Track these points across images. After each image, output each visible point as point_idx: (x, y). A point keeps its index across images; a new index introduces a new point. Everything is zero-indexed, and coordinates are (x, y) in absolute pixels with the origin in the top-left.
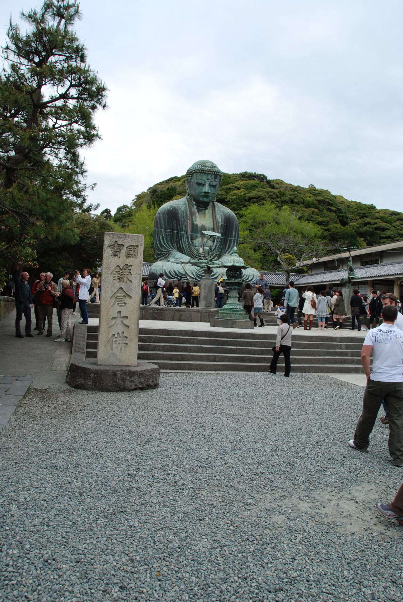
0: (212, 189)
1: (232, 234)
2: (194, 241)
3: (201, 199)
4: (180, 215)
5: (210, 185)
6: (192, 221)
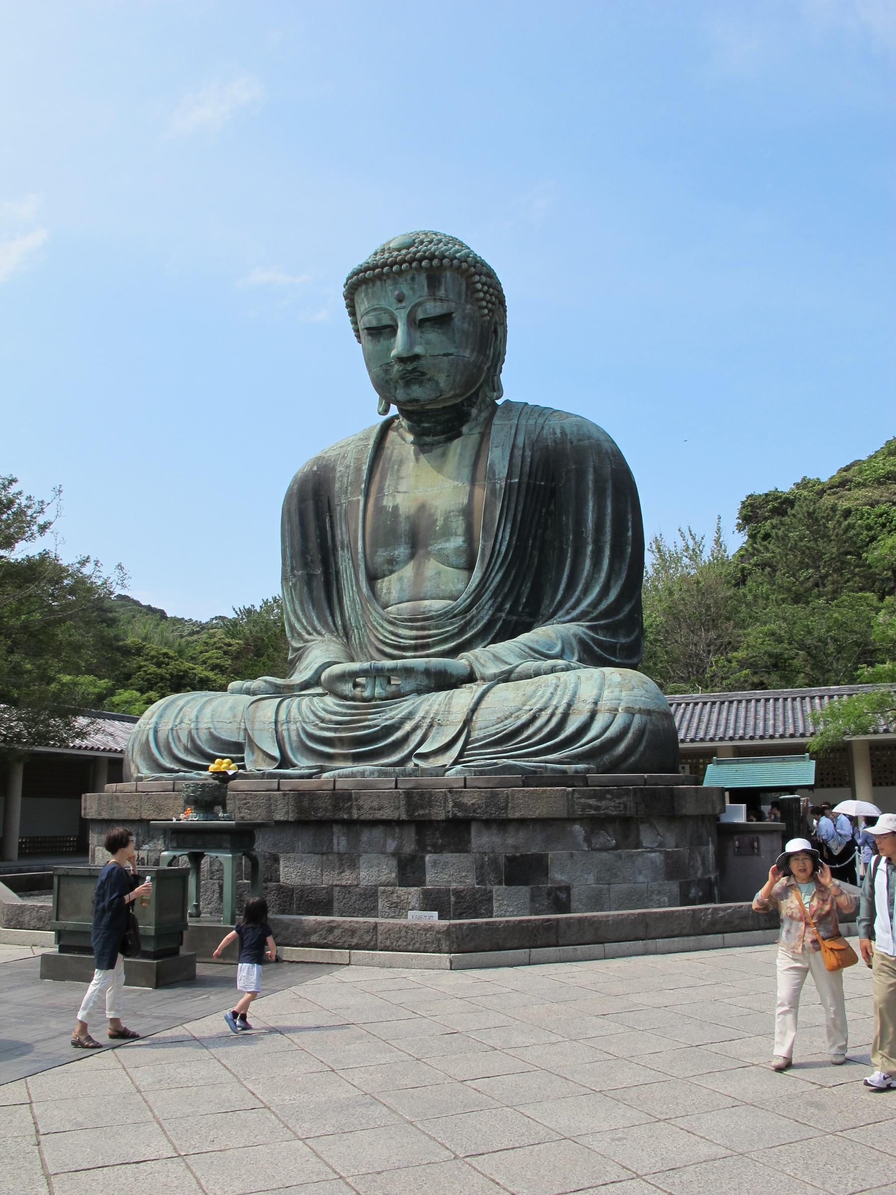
0: (433, 335)
1: (580, 522)
2: (383, 585)
4: (337, 485)
6: (379, 499)
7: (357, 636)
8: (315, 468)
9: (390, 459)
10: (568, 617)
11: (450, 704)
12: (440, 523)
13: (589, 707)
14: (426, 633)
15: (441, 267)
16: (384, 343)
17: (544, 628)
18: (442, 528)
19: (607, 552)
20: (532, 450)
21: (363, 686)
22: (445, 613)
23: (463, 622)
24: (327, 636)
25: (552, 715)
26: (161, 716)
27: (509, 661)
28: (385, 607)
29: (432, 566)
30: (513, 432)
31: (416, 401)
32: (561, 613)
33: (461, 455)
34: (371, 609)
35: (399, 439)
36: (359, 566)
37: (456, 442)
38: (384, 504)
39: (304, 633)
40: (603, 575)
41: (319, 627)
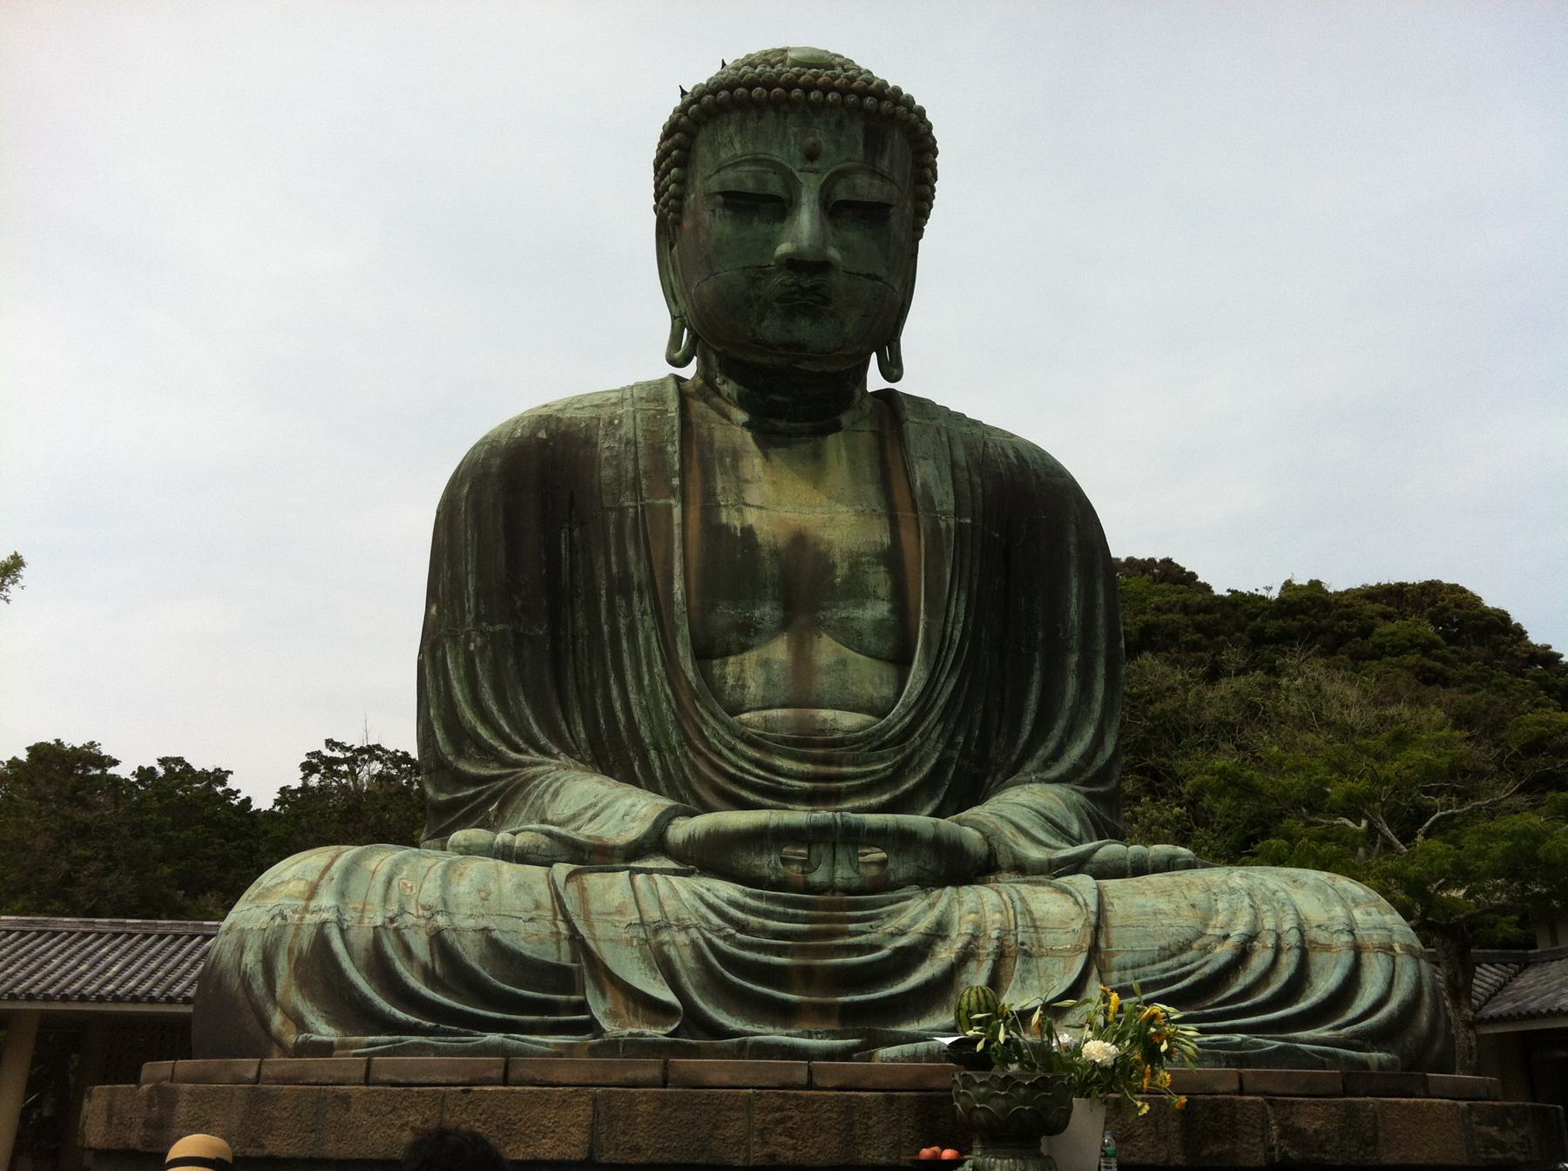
0: (854, 236)
3: (771, 329)
4: (607, 473)
5: (833, 210)
6: (710, 506)
7: (657, 764)
8: (542, 435)
9: (711, 443)
10: (1054, 773)
11: (1030, 912)
12: (842, 570)
13: (1345, 938)
14: (834, 770)
15: (892, 117)
16: (759, 227)
17: (1036, 787)
18: (847, 580)
19: (1101, 670)
20: (980, 475)
21: (803, 863)
22: (868, 736)
23: (899, 757)
24: (563, 757)
25: (1278, 950)
26: (342, 894)
27: (1042, 836)
28: (736, 709)
29: (827, 650)
30: (944, 439)
31: (800, 347)
32: (1030, 766)
33: (853, 462)
34: (706, 716)
35: (713, 414)
36: (675, 628)
37: (831, 438)
38: (724, 519)
39: (503, 748)
40: (1097, 708)
41: (543, 740)
